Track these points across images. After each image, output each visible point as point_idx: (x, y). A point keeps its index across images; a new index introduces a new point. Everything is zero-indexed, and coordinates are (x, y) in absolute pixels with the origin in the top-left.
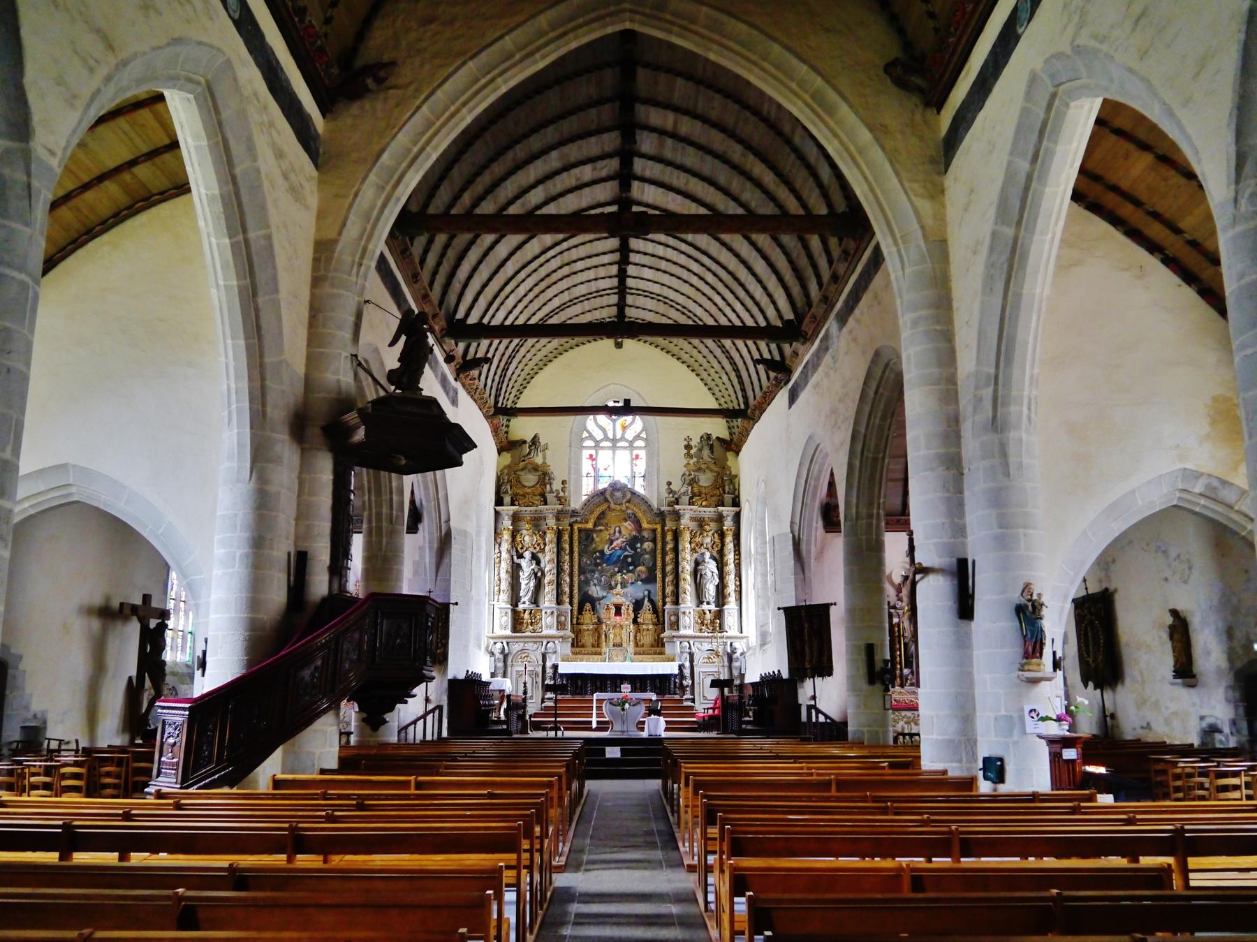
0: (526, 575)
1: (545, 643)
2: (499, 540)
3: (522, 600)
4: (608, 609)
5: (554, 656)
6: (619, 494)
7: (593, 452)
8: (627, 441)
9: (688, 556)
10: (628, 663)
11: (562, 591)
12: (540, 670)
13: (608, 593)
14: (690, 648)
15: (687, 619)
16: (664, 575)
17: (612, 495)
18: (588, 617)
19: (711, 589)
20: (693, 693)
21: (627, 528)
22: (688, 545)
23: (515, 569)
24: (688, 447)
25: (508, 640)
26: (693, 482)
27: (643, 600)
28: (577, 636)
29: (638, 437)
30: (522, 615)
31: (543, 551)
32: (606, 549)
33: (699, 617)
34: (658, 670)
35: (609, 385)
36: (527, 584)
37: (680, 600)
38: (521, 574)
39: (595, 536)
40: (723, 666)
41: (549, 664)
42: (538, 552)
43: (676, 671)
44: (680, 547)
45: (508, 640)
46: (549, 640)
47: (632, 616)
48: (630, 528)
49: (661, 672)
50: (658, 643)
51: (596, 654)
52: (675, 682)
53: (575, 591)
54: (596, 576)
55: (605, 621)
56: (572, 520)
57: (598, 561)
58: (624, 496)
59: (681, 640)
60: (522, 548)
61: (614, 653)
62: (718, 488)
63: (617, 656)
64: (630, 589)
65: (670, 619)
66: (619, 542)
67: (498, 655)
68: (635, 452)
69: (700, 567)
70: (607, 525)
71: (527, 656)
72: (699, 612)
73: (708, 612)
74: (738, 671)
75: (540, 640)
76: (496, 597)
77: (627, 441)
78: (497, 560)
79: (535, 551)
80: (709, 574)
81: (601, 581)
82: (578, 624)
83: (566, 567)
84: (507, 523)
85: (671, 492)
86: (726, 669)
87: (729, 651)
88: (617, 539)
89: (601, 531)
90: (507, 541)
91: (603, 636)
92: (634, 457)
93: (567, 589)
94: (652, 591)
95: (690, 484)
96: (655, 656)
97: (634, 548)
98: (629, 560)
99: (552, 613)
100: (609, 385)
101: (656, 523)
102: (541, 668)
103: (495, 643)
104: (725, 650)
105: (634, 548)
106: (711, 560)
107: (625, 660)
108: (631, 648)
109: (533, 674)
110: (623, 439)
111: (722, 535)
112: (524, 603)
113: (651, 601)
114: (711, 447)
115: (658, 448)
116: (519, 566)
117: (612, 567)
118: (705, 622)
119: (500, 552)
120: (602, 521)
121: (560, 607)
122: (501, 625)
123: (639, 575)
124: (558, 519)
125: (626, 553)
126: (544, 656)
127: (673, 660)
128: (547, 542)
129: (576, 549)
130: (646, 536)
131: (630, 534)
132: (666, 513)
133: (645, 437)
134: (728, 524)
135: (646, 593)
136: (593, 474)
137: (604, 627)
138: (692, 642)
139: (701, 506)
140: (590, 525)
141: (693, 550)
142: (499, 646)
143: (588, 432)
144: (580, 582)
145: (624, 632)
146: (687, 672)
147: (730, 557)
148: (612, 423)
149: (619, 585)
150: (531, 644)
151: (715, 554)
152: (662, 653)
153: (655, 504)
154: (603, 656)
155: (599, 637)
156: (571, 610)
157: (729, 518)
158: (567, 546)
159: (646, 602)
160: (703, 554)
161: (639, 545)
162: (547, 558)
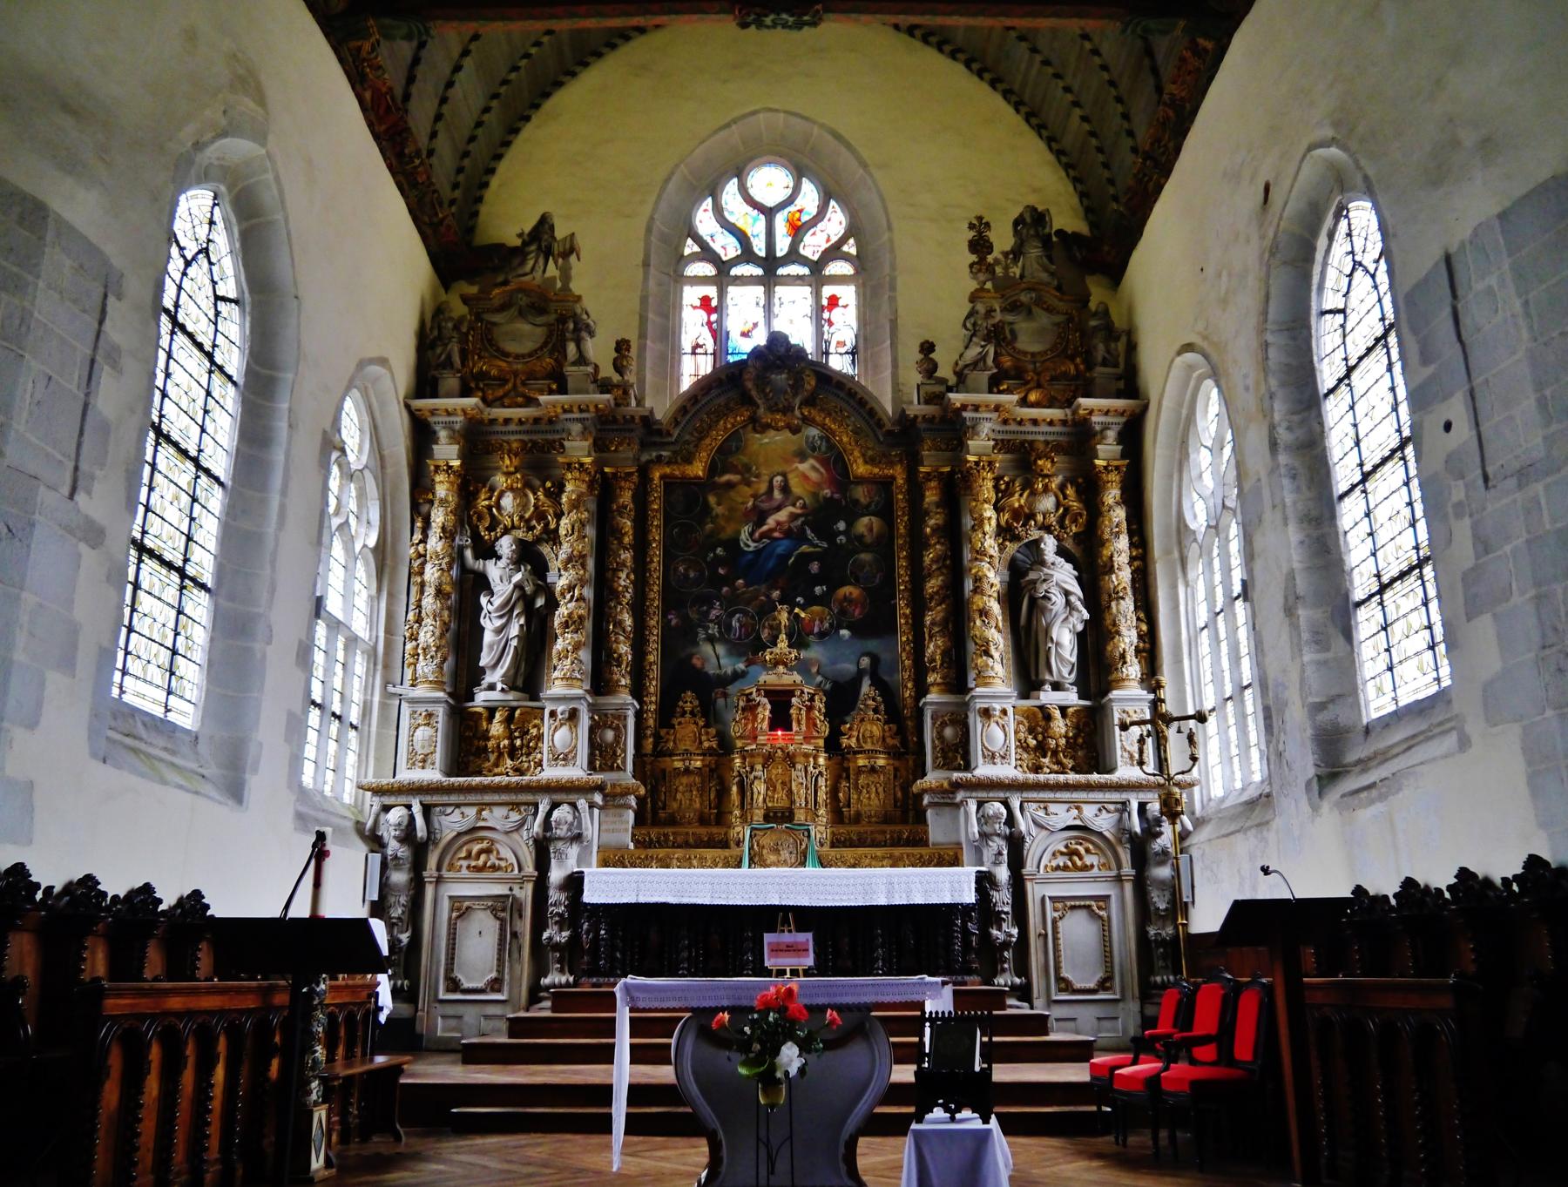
0: (497, 601)
1: (543, 808)
2: (425, 508)
3: (490, 678)
4: (751, 708)
5: (573, 851)
6: (780, 379)
7: (711, 291)
8: (804, 261)
9: (991, 545)
10: (811, 870)
11: (611, 652)
12: (526, 894)
13: (750, 663)
14: (1011, 821)
15: (998, 734)
16: (919, 605)
17: (762, 381)
18: (687, 732)
19: (1064, 638)
20: (1022, 968)
21: (805, 477)
22: (989, 512)
23: (470, 587)
24: (980, 245)
25: (428, 799)
26: (998, 336)
27: (856, 682)
28: (653, 791)
29: (833, 252)
30: (484, 724)
31: (553, 537)
32: (744, 536)
33: (1031, 731)
34: (909, 893)
35: (754, 113)
36: (499, 631)
37: (972, 675)
38: (483, 600)
39: (712, 500)
40: (1119, 879)
41: (556, 875)
42: (538, 540)
43: (969, 897)
44: (968, 522)
45: (428, 799)
46: (558, 797)
47: (825, 729)
48: (813, 476)
49: (919, 899)
50: (905, 812)
51: (711, 843)
52: (966, 933)
53: (651, 658)
54: (714, 613)
55: (739, 744)
56: (645, 458)
57: (721, 571)
58: (797, 386)
59: (983, 795)
60: (491, 528)
61: (767, 840)
62: (1072, 358)
63: (776, 851)
64: (815, 653)
65: (940, 736)
66: (782, 515)
67: (393, 846)
68: (828, 291)
69: (1032, 576)
70: (747, 468)
71: (488, 851)
72: (1029, 715)
73: (1057, 713)
74: (1168, 896)
75: (529, 798)
76: (409, 673)
77: (804, 261)
78: (416, 564)
79: (530, 537)
80: (1058, 600)
81: (729, 627)
82: (660, 752)
83: (624, 580)
84: (447, 452)
85: (929, 369)
86: (1128, 887)
87: (1138, 829)
88: (779, 508)
89: (730, 486)
90: (443, 502)
91: (735, 789)
92: (825, 302)
93: (624, 649)
94: (885, 656)
95: (987, 339)
96: (897, 851)
97: (829, 535)
98: (815, 567)
99: (573, 715)
100: (754, 113)
101: (891, 464)
102: (529, 887)
103: (386, 809)
104: (1122, 829)
105: (827, 534)
106: (1060, 560)
107: (803, 864)
108: (820, 830)
109: (503, 907)
110: (794, 256)
111: (1088, 486)
112: (492, 687)
113: (877, 683)
114: (1046, 242)
115: (893, 267)
116: (481, 583)
117: (763, 588)
118: (1052, 743)
119: (424, 541)
120: (733, 460)
121: (602, 700)
122: (412, 752)
123: (843, 612)
124: (599, 446)
125: (805, 548)
126: (542, 851)
127: (955, 861)
128: (565, 508)
129: (656, 535)
130: (863, 500)
131: (815, 495)
132: (921, 425)
133: (853, 251)
134: (1107, 451)
135: (865, 662)
136: (710, 347)
137: (738, 762)
138: (1015, 804)
139: (1024, 402)
140: (698, 469)
141: (1005, 533)
142: (396, 815)
143: (698, 240)
144: (666, 627)
145: (797, 774)
146: (1002, 899)
147: (1120, 548)
148: (762, 217)
149: (783, 636)
150: (500, 812)
151: (1069, 544)
152: (922, 841)
153: (887, 404)
154: (735, 851)
155: (723, 792)
156: (639, 715)
157: (1111, 435)
158: (627, 524)
159: (866, 687)
160: (1035, 545)
161: (842, 526)
162: (565, 550)
